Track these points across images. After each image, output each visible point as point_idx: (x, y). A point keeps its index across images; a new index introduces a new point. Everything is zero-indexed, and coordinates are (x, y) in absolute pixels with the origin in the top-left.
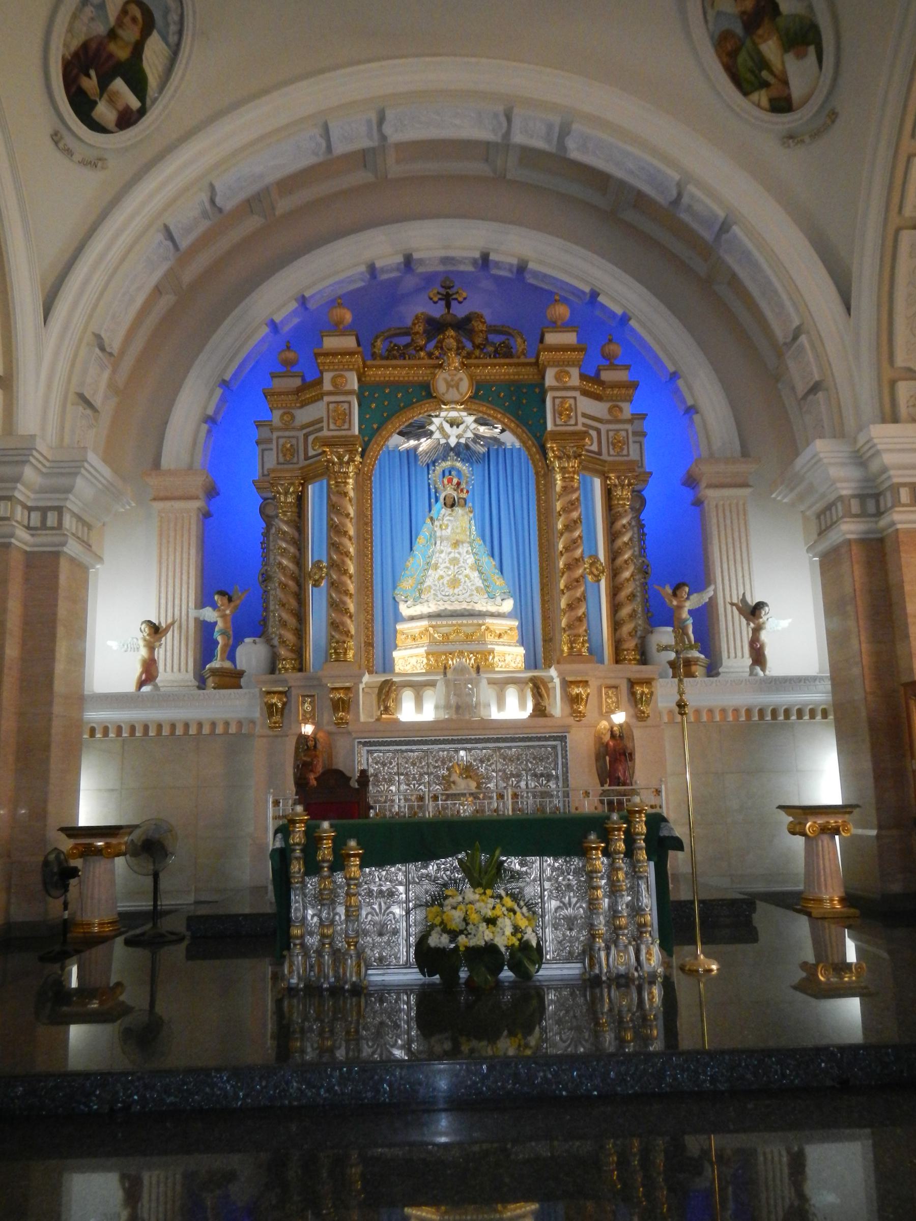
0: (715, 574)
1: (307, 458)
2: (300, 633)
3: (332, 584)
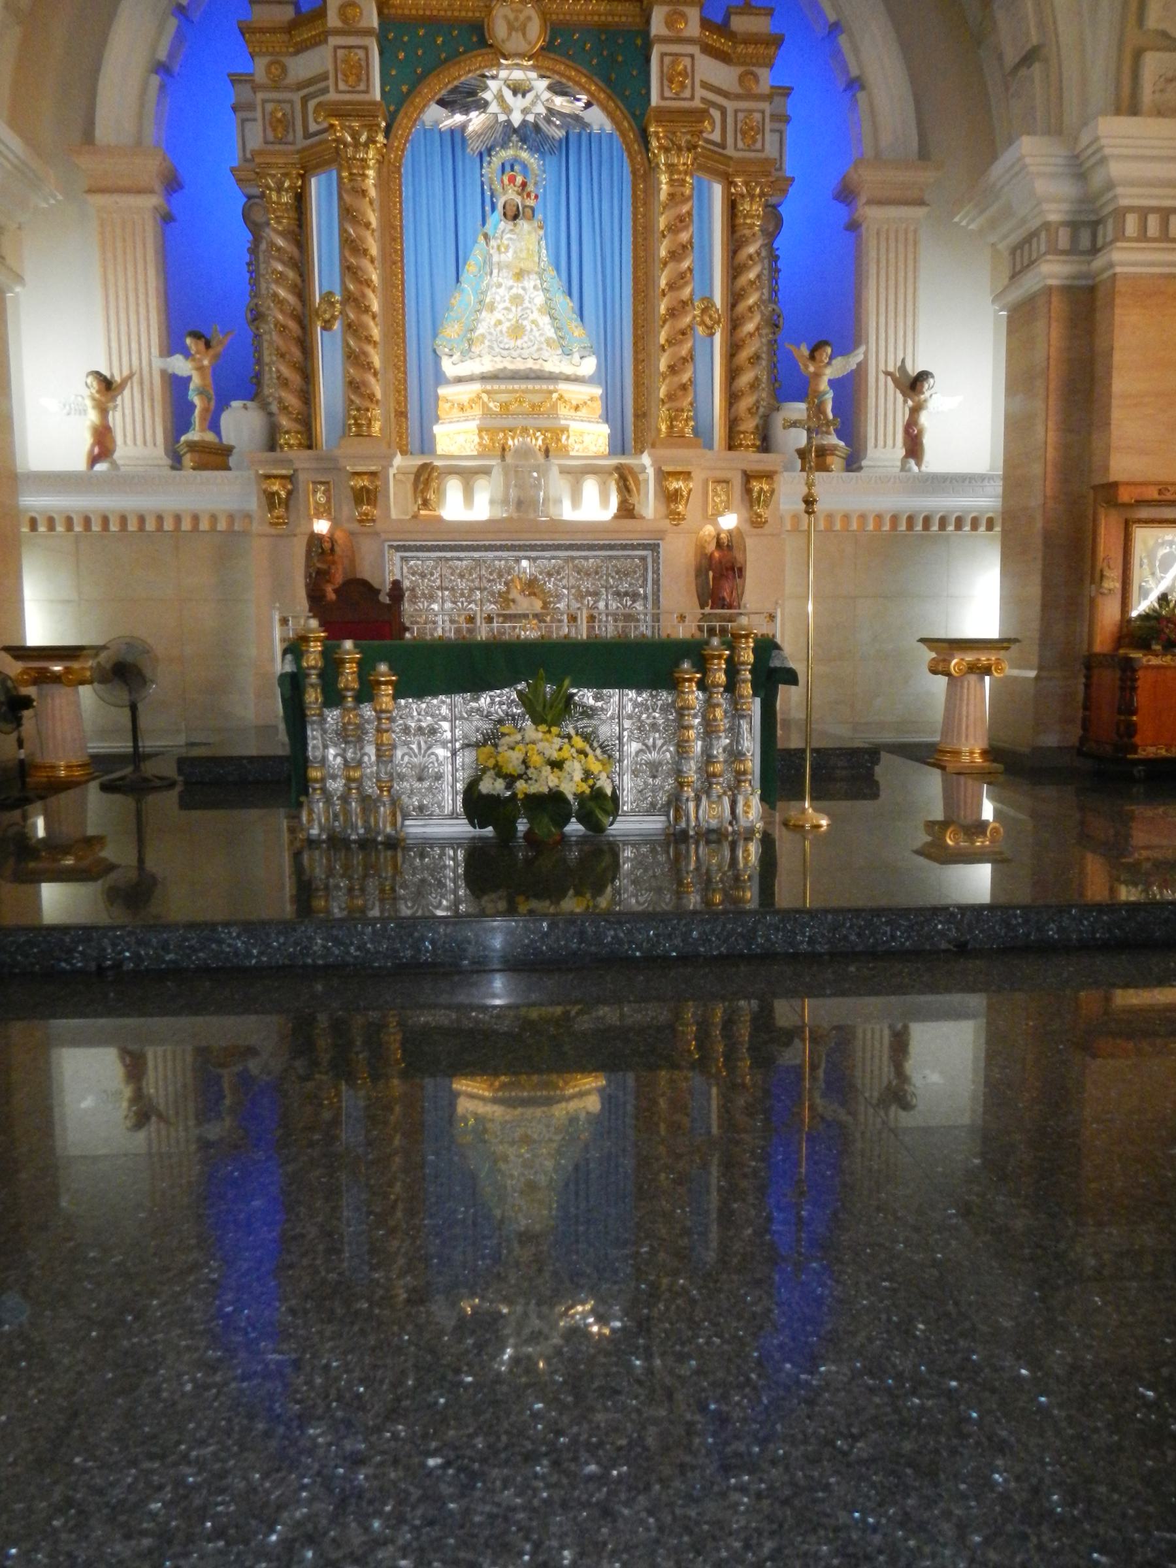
0: (867, 330)
1: (307, 135)
2: (307, 396)
3: (349, 326)
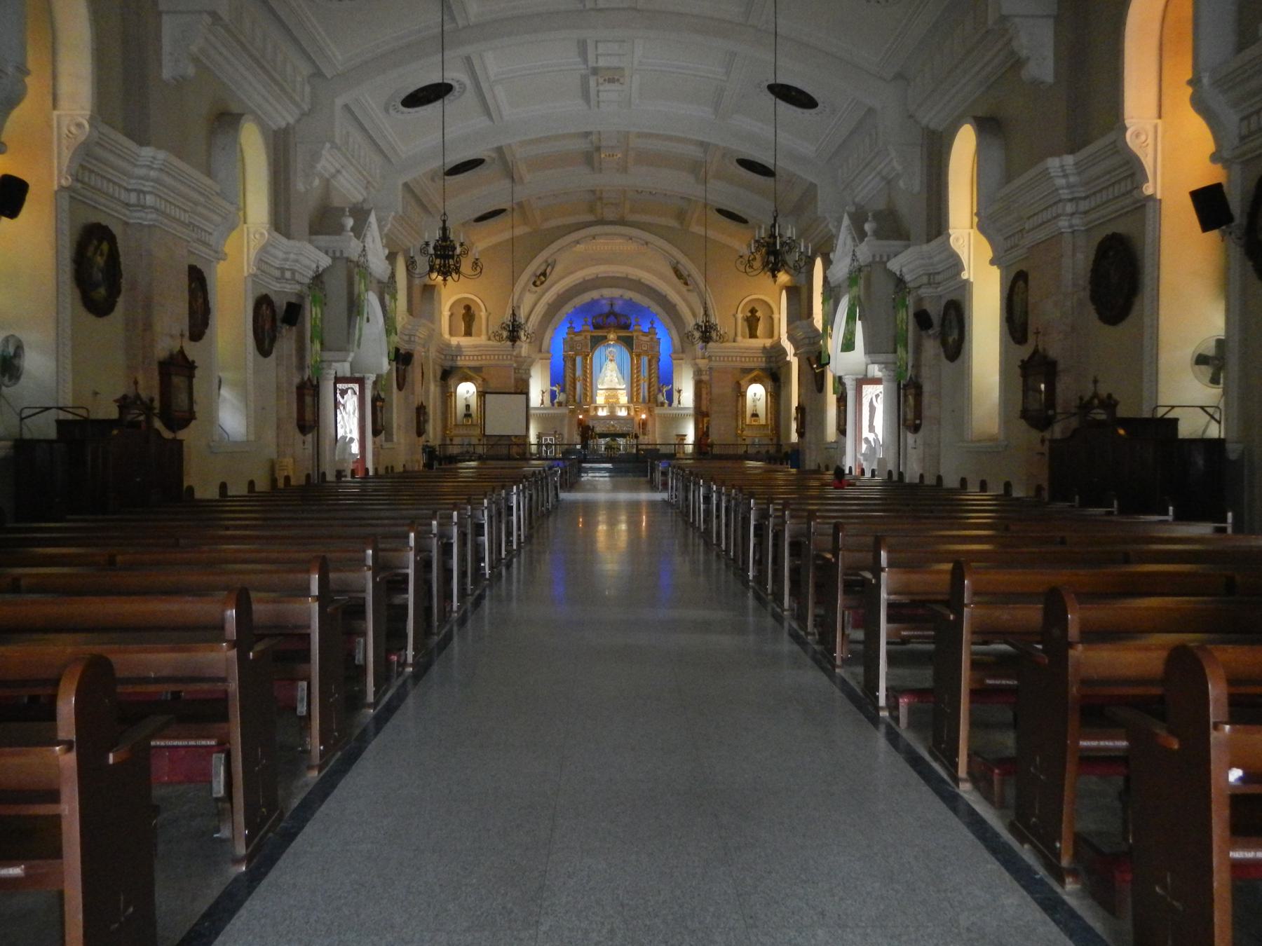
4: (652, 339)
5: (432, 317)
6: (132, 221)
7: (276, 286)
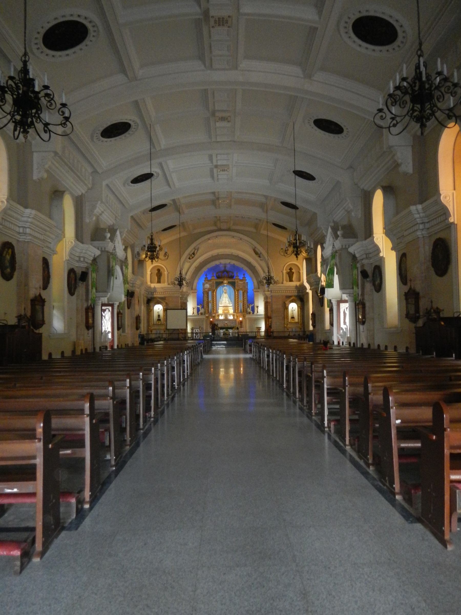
2: (208, 308)
4: (244, 282)
5: (143, 275)
6: (20, 240)
7: (77, 265)
